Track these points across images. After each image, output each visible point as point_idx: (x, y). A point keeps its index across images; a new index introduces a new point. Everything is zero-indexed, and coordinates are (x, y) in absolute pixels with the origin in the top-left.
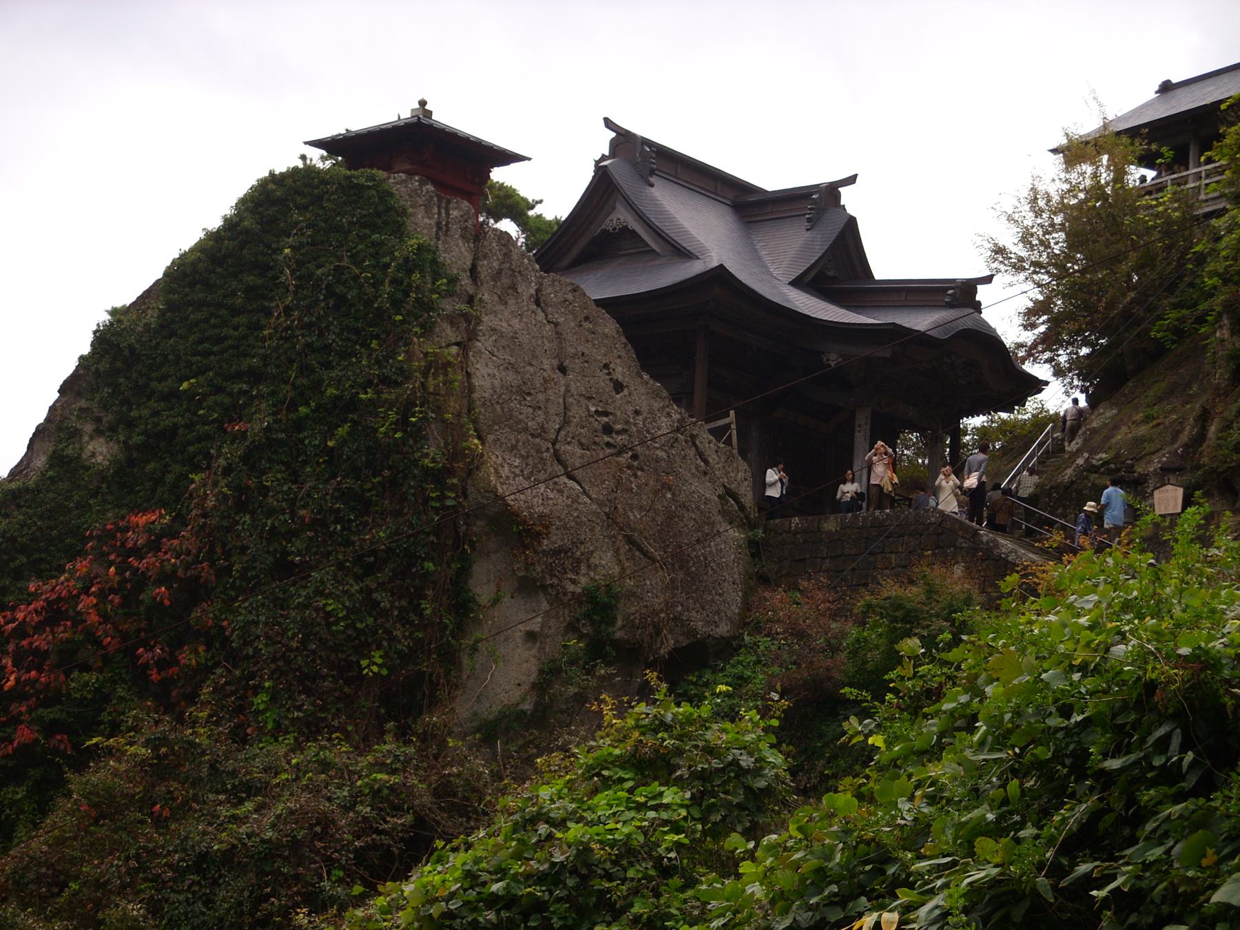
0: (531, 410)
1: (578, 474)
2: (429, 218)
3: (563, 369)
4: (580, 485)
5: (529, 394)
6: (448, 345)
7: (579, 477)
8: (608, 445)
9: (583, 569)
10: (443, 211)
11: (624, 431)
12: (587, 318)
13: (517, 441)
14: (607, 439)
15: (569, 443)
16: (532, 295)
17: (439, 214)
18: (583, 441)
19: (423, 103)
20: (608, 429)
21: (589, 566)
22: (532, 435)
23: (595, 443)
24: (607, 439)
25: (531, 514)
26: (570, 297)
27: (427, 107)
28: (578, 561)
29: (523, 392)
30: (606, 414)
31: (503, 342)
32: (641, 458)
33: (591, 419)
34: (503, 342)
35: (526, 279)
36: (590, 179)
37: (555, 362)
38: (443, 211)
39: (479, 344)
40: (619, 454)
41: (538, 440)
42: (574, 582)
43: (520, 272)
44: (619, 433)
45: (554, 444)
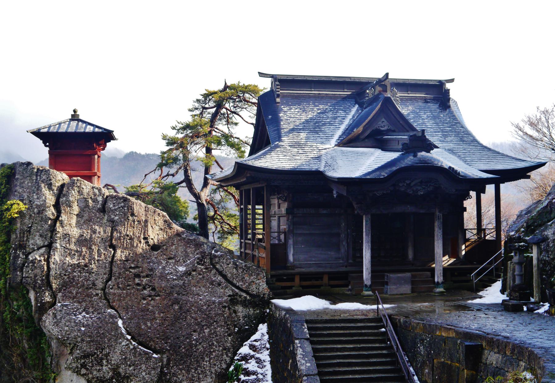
0: (88, 274)
4: (116, 311)
6: (39, 249)
8: (138, 284)
9: (104, 362)
10: (39, 177)
13: (77, 293)
14: (137, 281)
15: (112, 289)
16: (99, 209)
18: (121, 286)
19: (75, 111)
20: (138, 276)
21: (107, 361)
23: (129, 285)
24: (137, 281)
27: (77, 113)
28: (102, 359)
32: (157, 290)
40: (144, 288)
42: (99, 371)
44: (144, 277)
45: (103, 289)
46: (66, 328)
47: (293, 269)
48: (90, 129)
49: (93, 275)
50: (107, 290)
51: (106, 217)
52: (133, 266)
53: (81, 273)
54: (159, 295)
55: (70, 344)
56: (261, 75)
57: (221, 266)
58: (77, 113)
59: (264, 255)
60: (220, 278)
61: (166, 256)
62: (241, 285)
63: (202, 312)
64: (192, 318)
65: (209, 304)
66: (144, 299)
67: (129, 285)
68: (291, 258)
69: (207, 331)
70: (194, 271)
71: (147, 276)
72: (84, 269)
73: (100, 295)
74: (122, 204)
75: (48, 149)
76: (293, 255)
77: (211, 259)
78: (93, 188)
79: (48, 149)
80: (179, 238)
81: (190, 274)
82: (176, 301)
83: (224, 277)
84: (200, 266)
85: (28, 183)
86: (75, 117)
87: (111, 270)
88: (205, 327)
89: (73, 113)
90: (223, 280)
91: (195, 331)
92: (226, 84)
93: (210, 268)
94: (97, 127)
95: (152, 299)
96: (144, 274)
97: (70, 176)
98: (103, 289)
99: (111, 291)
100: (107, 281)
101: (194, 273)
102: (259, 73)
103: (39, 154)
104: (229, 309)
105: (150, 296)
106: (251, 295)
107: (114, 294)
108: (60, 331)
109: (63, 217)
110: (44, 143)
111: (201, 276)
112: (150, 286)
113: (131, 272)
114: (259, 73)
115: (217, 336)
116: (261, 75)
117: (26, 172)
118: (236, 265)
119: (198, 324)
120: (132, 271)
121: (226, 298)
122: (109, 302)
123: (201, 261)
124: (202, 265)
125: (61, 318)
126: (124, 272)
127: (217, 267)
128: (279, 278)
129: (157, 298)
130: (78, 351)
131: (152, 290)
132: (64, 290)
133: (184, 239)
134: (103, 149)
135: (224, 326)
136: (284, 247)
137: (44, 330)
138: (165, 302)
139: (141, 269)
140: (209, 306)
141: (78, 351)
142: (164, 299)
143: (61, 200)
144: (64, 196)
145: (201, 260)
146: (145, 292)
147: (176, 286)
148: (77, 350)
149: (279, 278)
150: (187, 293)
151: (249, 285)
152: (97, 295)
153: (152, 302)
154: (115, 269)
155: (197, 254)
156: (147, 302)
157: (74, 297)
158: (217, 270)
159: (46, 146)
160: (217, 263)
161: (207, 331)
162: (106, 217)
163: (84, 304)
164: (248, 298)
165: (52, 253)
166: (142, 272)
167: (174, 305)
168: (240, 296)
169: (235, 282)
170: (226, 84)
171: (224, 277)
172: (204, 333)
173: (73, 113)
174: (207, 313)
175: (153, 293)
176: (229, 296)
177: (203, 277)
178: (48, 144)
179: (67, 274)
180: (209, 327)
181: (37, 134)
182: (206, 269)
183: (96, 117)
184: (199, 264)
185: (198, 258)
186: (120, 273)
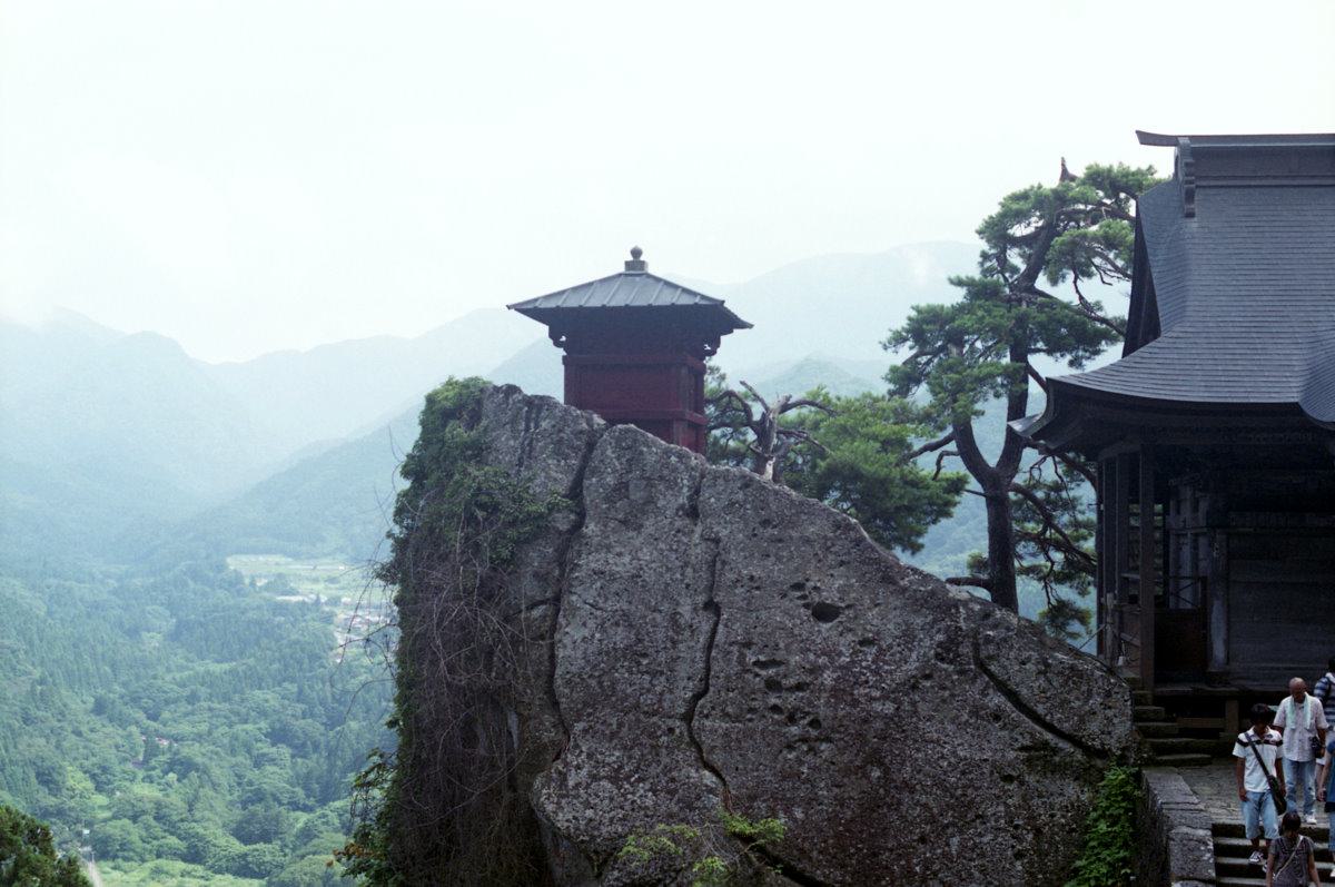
1: (717, 759)
2: (515, 438)
3: (712, 607)
4: (718, 775)
5: (645, 655)
7: (718, 765)
8: (775, 709)
10: (532, 425)
11: (799, 687)
12: (766, 523)
13: (620, 725)
14: (773, 700)
15: (707, 717)
16: (682, 507)
17: (527, 429)
18: (730, 710)
19: (636, 253)
20: (773, 685)
22: (645, 713)
23: (751, 710)
25: (593, 838)
26: (740, 496)
27: (642, 258)
29: (634, 653)
30: (773, 663)
31: (615, 587)
32: (824, 724)
33: (749, 676)
34: (615, 587)
35: (672, 485)
36: (742, 319)
37: (701, 599)
38: (532, 425)
39: (574, 598)
40: (792, 719)
41: (655, 719)
43: (661, 478)
44: (793, 689)
46: (589, 813)
47: (1227, 684)
48: (667, 298)
49: (663, 679)
50: (695, 723)
51: (698, 529)
52: (762, 658)
53: (631, 673)
54: (828, 740)
55: (596, 852)
56: (1147, 139)
57: (1004, 667)
58: (642, 258)
59: (1137, 642)
60: (996, 700)
61: (855, 635)
62: (1059, 720)
63: (946, 790)
64: (918, 803)
65: (966, 768)
66: (790, 747)
67: (751, 710)
68: (1219, 650)
69: (955, 841)
70: (928, 677)
71: (799, 687)
72: (639, 664)
73: (677, 731)
74: (740, 496)
75: (561, 352)
76: (1227, 642)
77: (976, 647)
78: (668, 453)
79: (561, 352)
80: (892, 588)
81: (914, 687)
82: (875, 758)
83: (1013, 696)
84: (945, 666)
85: (507, 439)
86: (636, 265)
87: (708, 669)
88: (950, 831)
89: (630, 258)
90: (1009, 706)
91: (923, 840)
92: (1064, 171)
93: (971, 670)
94: (686, 291)
95: (811, 749)
96: (792, 681)
97: (611, 422)
98: (688, 718)
99: (707, 723)
100: (698, 696)
101: (928, 684)
102: (1139, 133)
103: (541, 369)
104: (1022, 783)
105: (804, 740)
106: (1087, 750)
107: (713, 731)
108: (575, 818)
109: (591, 528)
110: (554, 336)
111: (947, 693)
112: (808, 713)
113: (757, 675)
114: (1139, 133)
115: (982, 855)
116: (1147, 139)
117: (504, 412)
118: (1048, 666)
119: (932, 820)
120: (763, 673)
121: (1011, 755)
122: (700, 750)
123: (947, 651)
124: (951, 662)
125: (577, 785)
126: (739, 676)
127: (992, 668)
128: (1174, 706)
129: (824, 746)
130: (616, 873)
131: (811, 724)
132: (589, 715)
133: (904, 590)
134: (713, 353)
135: (1005, 830)
136: (1201, 617)
137: (540, 815)
138: (846, 758)
139: (783, 668)
140: (963, 773)
141: (616, 873)
142: (842, 751)
143: (586, 483)
144: (593, 474)
145: (948, 650)
146: (794, 730)
147: (879, 716)
148: (613, 869)
149: (1174, 706)
150: (906, 737)
151: (1082, 720)
152: (671, 730)
153: (809, 757)
154: (715, 668)
155: (939, 631)
156: (797, 757)
157: (613, 735)
158: (992, 676)
159: (557, 344)
160: (990, 658)
161: (955, 841)
162: (698, 529)
163: (637, 753)
164: (1079, 756)
165: (561, 620)
166: (785, 676)
167: (869, 766)
168: (1055, 751)
169: (1040, 709)
170: (1064, 171)
171: (1013, 696)
172: (948, 845)
173: (630, 258)
174: (959, 792)
175: (814, 733)
176: (1023, 749)
177: (953, 695)
178: (564, 339)
179: (597, 674)
180: (961, 832)
181: (531, 310)
182: (961, 673)
183: (690, 266)
184: (942, 660)
185: (940, 644)
186: (728, 678)
